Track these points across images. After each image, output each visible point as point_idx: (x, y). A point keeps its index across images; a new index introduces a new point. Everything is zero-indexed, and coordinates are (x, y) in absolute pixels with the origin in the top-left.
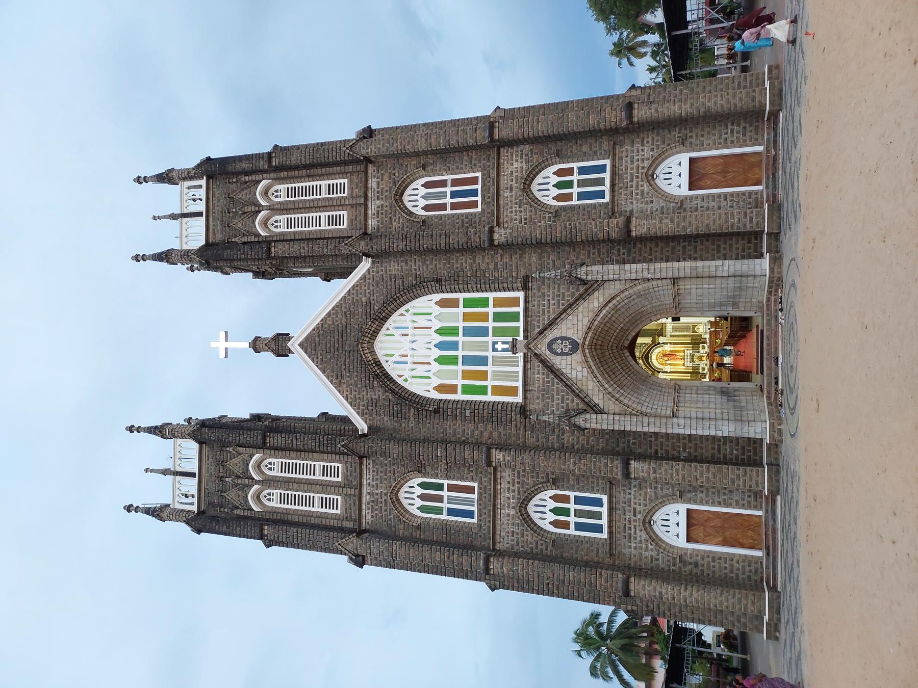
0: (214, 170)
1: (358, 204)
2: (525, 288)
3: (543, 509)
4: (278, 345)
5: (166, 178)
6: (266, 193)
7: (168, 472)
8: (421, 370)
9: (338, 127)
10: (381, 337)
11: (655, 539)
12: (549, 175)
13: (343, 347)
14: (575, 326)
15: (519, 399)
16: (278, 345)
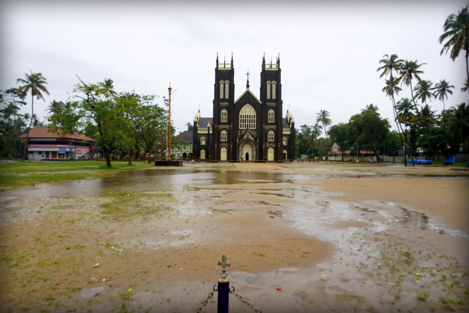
0: (278, 72)
1: (271, 100)
2: (256, 129)
3: (224, 132)
4: (248, 86)
5: (278, 62)
6: (274, 83)
7: (225, 64)
8: (244, 112)
9: (284, 97)
10: (249, 105)
11: (222, 147)
12: (273, 133)
13: (248, 98)
14: (250, 137)
15: (240, 128)
16: (248, 86)
